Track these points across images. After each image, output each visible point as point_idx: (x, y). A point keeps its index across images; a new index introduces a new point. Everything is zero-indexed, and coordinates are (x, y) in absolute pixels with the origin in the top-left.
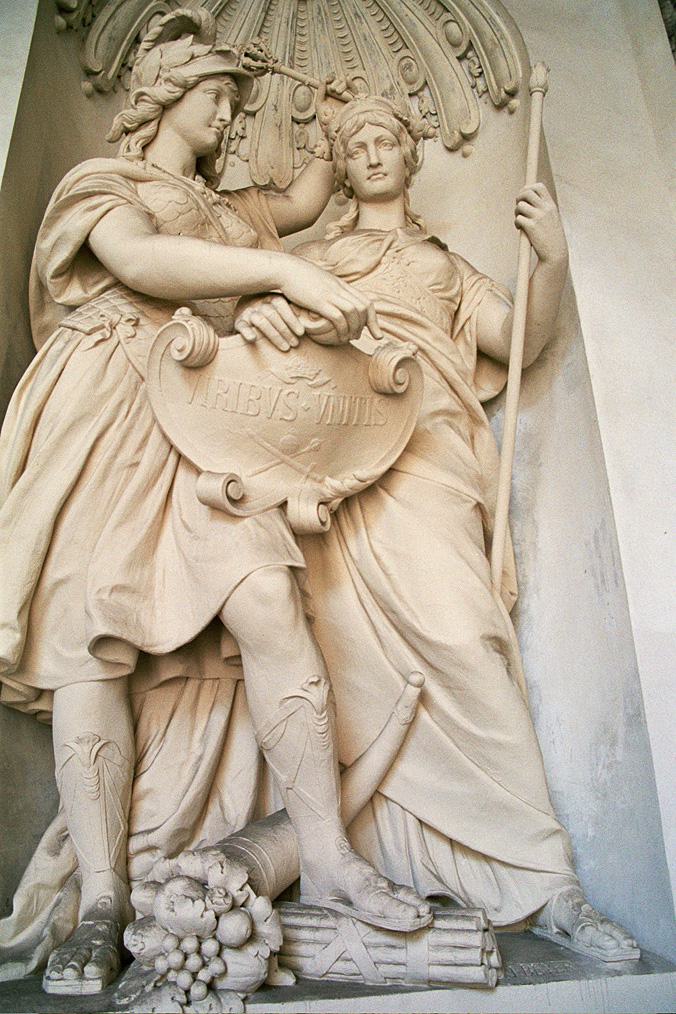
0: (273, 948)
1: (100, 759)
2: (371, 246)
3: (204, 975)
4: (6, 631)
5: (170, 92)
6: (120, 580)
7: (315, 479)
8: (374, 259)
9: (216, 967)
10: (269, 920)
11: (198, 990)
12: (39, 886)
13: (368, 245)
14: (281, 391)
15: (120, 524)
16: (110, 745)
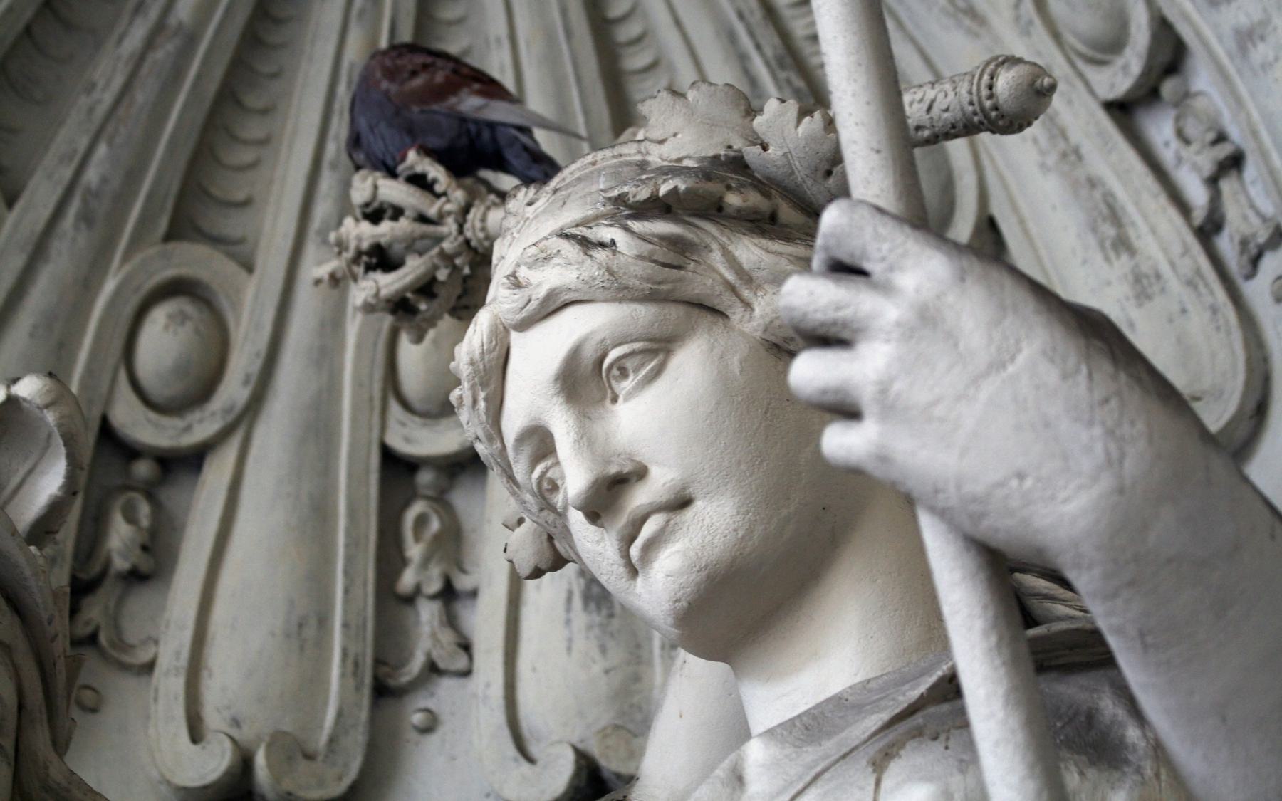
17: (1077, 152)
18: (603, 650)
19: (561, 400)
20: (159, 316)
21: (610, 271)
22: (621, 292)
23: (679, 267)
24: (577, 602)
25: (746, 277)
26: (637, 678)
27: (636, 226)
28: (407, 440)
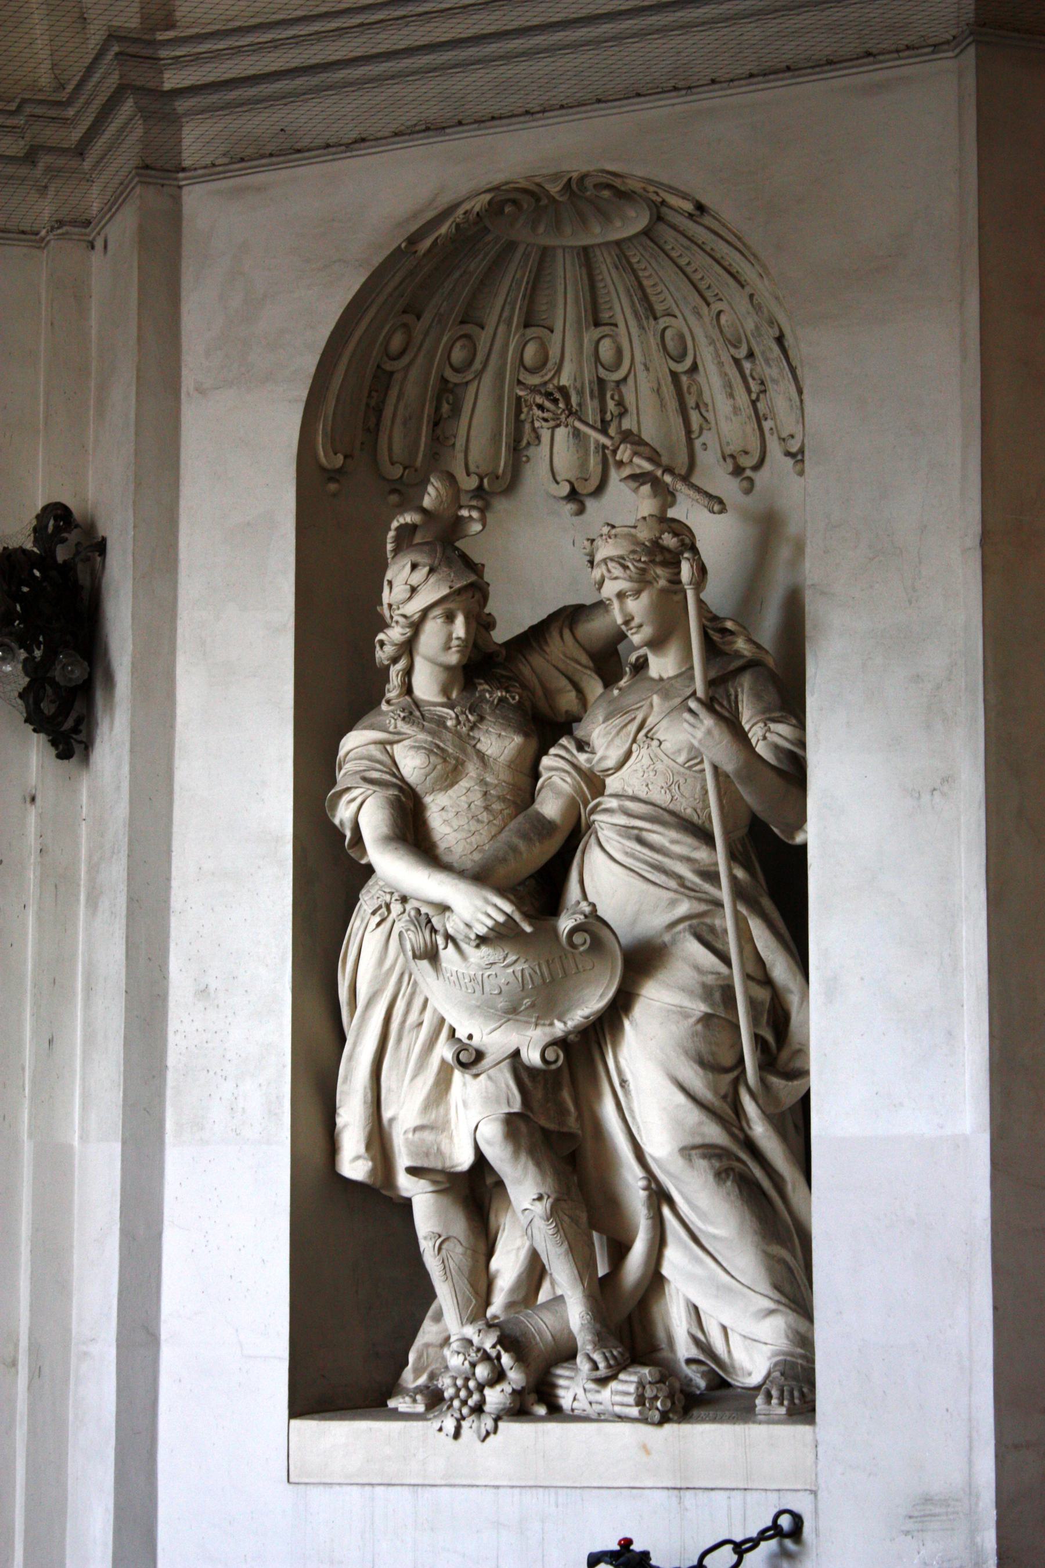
0: (514, 1387)
1: (443, 1252)
2: (622, 734)
3: (471, 1402)
4: (360, 1162)
6: (418, 1122)
7: (544, 1025)
9: (476, 1397)
11: (465, 1411)
12: (427, 1345)
13: (618, 733)
14: (482, 975)
15: (415, 1076)
16: (452, 1240)
17: (723, 363)
18: (577, 451)
20: (458, 345)
22: (631, 579)
24: (571, 436)
25: (658, 576)
27: (636, 564)
28: (525, 379)
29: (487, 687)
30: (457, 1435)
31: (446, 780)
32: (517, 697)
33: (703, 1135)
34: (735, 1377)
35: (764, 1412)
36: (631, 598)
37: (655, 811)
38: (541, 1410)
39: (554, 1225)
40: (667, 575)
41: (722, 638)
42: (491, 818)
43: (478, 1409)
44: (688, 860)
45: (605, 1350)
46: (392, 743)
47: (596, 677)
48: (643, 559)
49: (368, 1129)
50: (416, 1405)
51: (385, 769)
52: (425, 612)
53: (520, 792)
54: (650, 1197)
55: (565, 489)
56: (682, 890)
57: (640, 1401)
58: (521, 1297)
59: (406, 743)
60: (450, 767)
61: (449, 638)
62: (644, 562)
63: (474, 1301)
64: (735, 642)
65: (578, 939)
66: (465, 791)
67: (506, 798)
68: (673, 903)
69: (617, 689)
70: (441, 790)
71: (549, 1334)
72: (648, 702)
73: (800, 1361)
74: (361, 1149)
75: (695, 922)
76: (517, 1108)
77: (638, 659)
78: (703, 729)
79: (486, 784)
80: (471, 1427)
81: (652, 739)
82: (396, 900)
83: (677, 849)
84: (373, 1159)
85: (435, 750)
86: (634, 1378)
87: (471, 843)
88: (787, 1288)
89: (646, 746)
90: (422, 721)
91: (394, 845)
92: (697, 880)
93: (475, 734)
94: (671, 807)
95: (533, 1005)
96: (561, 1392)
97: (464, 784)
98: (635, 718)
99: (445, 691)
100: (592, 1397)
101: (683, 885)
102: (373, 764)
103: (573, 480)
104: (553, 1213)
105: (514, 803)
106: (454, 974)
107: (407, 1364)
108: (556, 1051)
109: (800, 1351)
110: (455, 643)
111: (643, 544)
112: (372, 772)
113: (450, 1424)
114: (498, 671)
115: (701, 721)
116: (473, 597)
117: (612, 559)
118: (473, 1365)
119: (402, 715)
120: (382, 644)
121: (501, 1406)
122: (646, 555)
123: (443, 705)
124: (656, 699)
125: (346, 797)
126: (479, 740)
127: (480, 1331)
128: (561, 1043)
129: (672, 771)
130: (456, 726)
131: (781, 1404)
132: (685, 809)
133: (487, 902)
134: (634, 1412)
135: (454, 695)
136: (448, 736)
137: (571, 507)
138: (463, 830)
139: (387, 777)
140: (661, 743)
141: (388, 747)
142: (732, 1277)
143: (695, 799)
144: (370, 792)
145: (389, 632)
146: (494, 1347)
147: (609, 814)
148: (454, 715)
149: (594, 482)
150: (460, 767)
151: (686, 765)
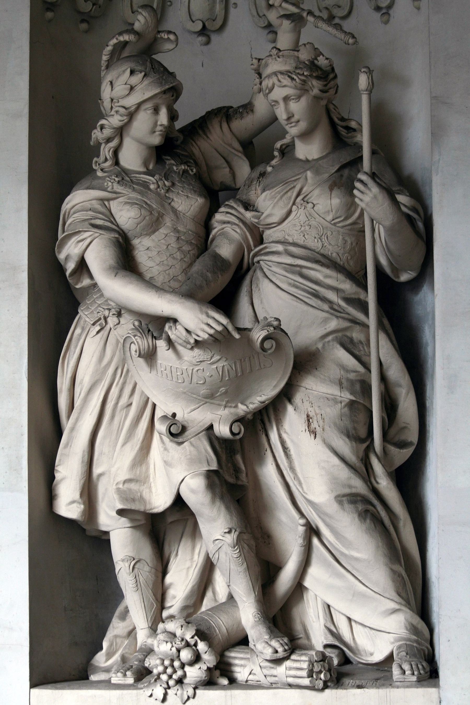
0: (209, 665)
1: (136, 570)
2: (284, 198)
3: (175, 677)
4: (75, 505)
5: (121, 121)
6: (127, 477)
7: (231, 407)
8: (285, 211)
9: (180, 673)
10: (207, 653)
11: (171, 683)
12: (116, 636)
13: (281, 197)
14: (193, 369)
15: (124, 444)
16: (142, 561)
19: (283, 100)
21: (295, 86)
22: (296, 88)
23: (304, 85)
25: (313, 86)
26: (214, 6)
27: (299, 77)
29: (173, 162)
30: (164, 700)
31: (151, 228)
32: (194, 170)
33: (350, 487)
34: (360, 656)
35: (401, 680)
36: (294, 101)
37: (312, 254)
38: (225, 682)
39: (238, 551)
40: (320, 86)
41: (347, 134)
42: (183, 257)
43: (180, 681)
44: (336, 290)
45: (279, 639)
46: (109, 200)
47: (245, 159)
48: (305, 73)
49: (82, 481)
50: (126, 679)
51: (106, 219)
52: (139, 106)
53: (199, 238)
54: (306, 531)
55: (199, 26)
56: (332, 311)
57: (310, 675)
58: (192, 602)
59: (121, 199)
60: (155, 219)
61: (155, 124)
62: (306, 76)
63: (155, 606)
64: (356, 136)
65: (267, 345)
66: (164, 236)
67: (191, 242)
68: (325, 321)
69: (270, 166)
70: (147, 235)
71: (224, 628)
72: (304, 176)
73: (415, 645)
74: (77, 496)
75: (340, 334)
76: (214, 467)
77: (281, 146)
78: (371, 195)
79: (178, 232)
80: (176, 694)
81: (308, 203)
82: (114, 314)
83: (329, 281)
84: (84, 504)
85: (144, 206)
86: (306, 659)
87: (169, 274)
88: (404, 595)
89: (303, 208)
90: (132, 184)
91: (122, 273)
92: (342, 304)
93: (170, 195)
94: (322, 251)
95: (226, 393)
96: (236, 669)
97: (163, 231)
98: (294, 187)
99: (145, 164)
100: (266, 672)
101: (332, 308)
102: (95, 214)
103: (204, 20)
104: (239, 542)
105: (197, 246)
106: (168, 368)
107: (101, 649)
108: (239, 426)
109: (414, 637)
110: (159, 128)
111: (304, 63)
112: (97, 220)
113: (159, 691)
114: (178, 151)
115: (369, 189)
116: (173, 96)
117: (282, 73)
118: (179, 651)
119: (117, 179)
120: (102, 127)
121: (199, 679)
122: (307, 71)
123: (144, 173)
124: (309, 174)
125: (74, 239)
126: (173, 200)
127: (182, 626)
128: (240, 420)
129: (322, 227)
130: (157, 189)
131: (413, 674)
132: (332, 254)
133: (208, 316)
134: (306, 682)
135: (151, 167)
136: (153, 195)
137: (202, 39)
138: (163, 265)
139: (109, 224)
140: (314, 206)
141: (106, 203)
142: (367, 587)
143: (339, 247)
144: (97, 235)
145: (110, 119)
146: (193, 637)
147: (277, 255)
148: (155, 181)
149: (219, 22)
150: (160, 219)
151: (333, 222)
